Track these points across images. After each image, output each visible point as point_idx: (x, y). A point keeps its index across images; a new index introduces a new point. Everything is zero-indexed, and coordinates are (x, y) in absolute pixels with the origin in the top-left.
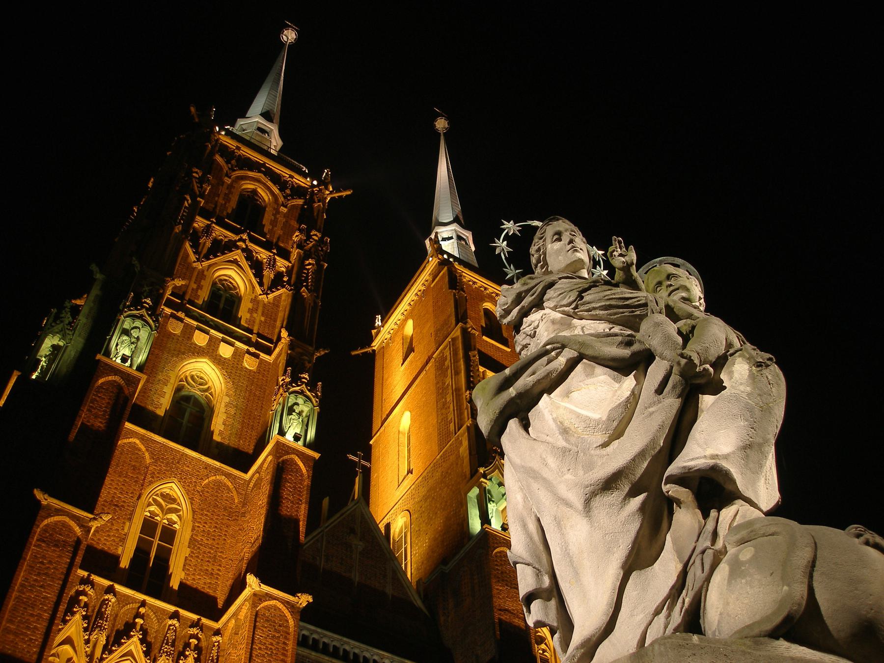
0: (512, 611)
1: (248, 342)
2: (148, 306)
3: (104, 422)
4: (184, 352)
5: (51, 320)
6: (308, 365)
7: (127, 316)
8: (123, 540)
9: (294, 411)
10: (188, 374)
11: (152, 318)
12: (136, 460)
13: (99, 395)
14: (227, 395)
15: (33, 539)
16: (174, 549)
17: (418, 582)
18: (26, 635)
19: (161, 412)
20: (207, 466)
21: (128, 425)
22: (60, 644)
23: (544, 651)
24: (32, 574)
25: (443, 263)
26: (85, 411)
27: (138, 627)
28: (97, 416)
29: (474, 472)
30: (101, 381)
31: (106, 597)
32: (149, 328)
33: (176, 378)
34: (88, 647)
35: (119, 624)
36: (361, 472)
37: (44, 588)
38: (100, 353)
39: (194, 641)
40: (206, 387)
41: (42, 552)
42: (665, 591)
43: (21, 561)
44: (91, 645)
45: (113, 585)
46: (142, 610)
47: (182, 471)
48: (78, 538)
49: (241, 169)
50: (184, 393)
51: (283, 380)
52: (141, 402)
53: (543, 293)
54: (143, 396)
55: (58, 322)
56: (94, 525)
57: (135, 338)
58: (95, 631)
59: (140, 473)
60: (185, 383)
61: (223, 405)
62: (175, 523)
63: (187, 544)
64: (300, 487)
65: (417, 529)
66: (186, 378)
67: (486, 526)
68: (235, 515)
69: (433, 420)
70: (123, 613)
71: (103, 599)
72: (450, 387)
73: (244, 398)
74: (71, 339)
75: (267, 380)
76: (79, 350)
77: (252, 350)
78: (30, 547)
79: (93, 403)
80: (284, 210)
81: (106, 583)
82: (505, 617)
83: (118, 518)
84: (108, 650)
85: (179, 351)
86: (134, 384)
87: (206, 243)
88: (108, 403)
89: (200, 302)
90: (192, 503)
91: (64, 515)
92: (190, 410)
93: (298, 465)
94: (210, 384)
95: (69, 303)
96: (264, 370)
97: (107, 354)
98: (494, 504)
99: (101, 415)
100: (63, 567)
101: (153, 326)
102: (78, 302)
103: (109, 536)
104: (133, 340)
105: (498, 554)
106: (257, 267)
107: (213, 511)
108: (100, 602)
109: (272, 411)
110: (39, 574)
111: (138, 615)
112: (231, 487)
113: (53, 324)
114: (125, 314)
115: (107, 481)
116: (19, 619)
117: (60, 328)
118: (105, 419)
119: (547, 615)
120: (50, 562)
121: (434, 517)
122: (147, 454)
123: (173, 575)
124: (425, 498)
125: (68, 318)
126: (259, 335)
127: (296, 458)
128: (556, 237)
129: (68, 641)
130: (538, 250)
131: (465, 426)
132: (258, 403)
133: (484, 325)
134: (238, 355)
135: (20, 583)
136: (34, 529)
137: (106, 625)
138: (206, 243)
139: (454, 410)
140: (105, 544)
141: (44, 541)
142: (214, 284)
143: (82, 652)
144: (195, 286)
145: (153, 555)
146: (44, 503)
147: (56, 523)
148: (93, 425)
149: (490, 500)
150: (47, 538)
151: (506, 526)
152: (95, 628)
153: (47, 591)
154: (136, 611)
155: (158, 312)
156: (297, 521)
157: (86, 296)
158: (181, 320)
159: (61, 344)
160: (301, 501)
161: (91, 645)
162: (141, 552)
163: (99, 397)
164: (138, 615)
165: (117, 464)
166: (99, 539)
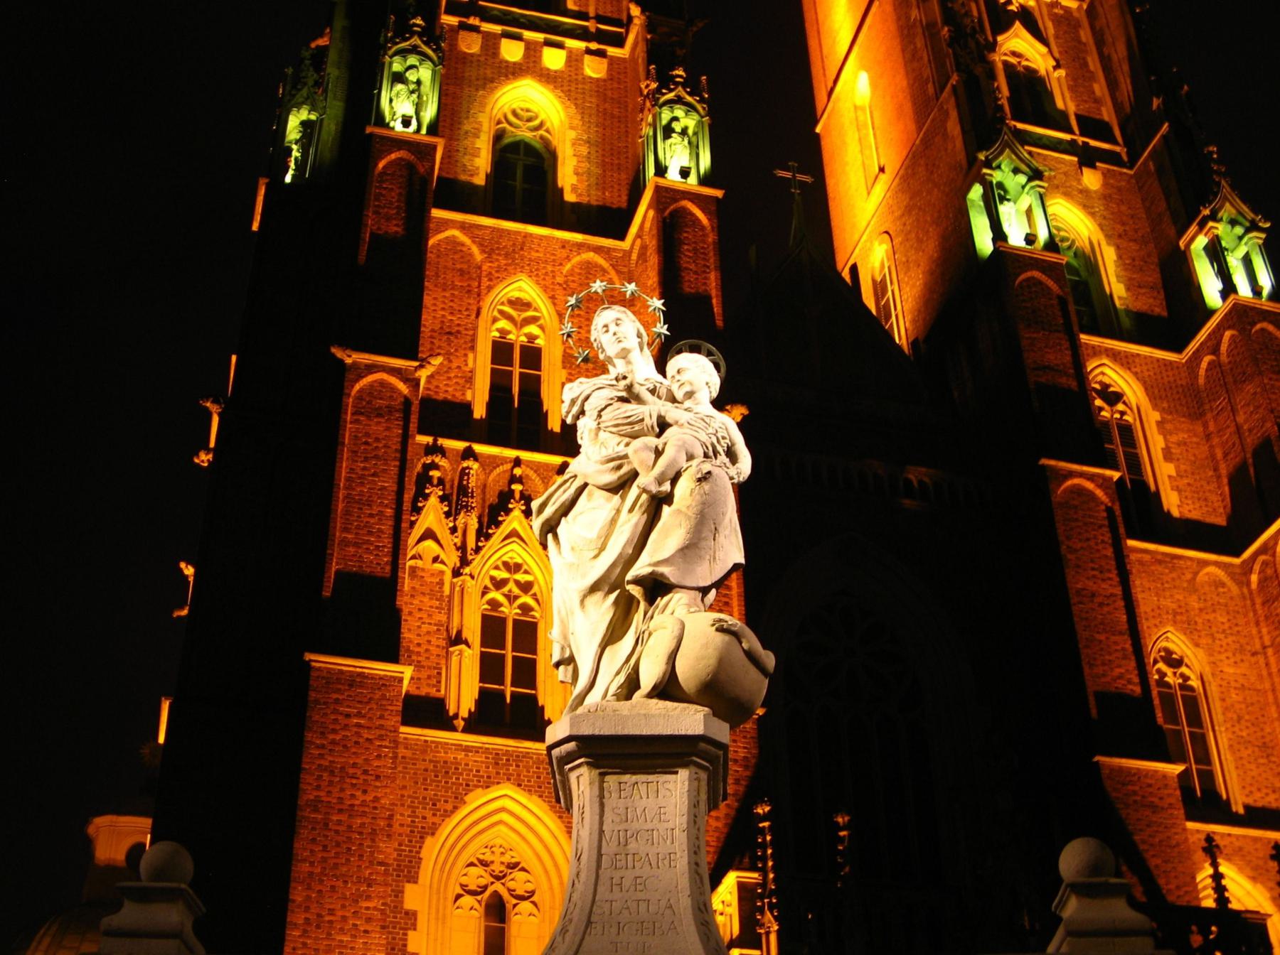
0: (1056, 368)
2: (419, 29)
3: (400, 223)
4: (493, 78)
5: (288, 88)
6: (680, 52)
7: (396, 54)
8: (469, 379)
9: (673, 131)
10: (506, 109)
11: (430, 47)
12: (461, 260)
13: (385, 186)
14: (572, 128)
15: (346, 413)
16: (544, 374)
17: (914, 344)
18: (368, 542)
19: (480, 180)
20: (564, 244)
21: (437, 213)
22: (419, 541)
23: (1123, 413)
24: (357, 461)
26: (370, 214)
27: (517, 496)
28: (388, 219)
29: (972, 160)
30: (381, 165)
31: (465, 464)
32: (430, 63)
33: (490, 122)
34: (456, 537)
35: (491, 496)
36: (799, 194)
37: (378, 477)
38: (370, 124)
40: (536, 123)
41: (363, 429)
42: (624, 659)
43: (340, 447)
44: (460, 533)
45: (470, 447)
46: (518, 471)
47: (530, 260)
48: (406, 398)
50: (507, 140)
51: (647, 86)
52: (448, 173)
53: (583, 405)
54: (449, 162)
55: (299, 87)
56: (423, 374)
57: (414, 83)
58: (460, 513)
59: (471, 279)
60: (505, 125)
61: (568, 145)
62: (537, 337)
63: (559, 364)
64: (703, 248)
65: (904, 259)
66: (506, 117)
67: (999, 243)
69: (902, 81)
70: (493, 480)
71: (460, 468)
72: (918, 24)
73: (597, 126)
74: (325, 107)
75: (626, 87)
76: (340, 120)
77: (594, 46)
78: (346, 426)
79: (378, 200)
81: (460, 445)
83: (456, 350)
84: (483, 534)
85: (485, 79)
86: (430, 155)
88: (400, 194)
90: (554, 304)
91: (379, 371)
93: (692, 214)
94: (542, 116)
95: (307, 51)
96: (619, 73)
97: (381, 121)
98: (1011, 204)
99: (394, 214)
100: (395, 444)
101: (435, 58)
102: (322, 42)
103: (449, 378)
104: (412, 87)
105: (1024, 284)
107: (588, 308)
108: (458, 474)
109: (641, 137)
110: (366, 459)
111: (514, 479)
113: (293, 92)
114: (390, 52)
115: (427, 300)
116: (356, 524)
117: (305, 95)
118: (401, 219)
119: (566, 676)
120: (377, 440)
121: (925, 239)
122: (475, 250)
123: (549, 412)
124: (909, 210)
125: (312, 76)
126: (600, 19)
128: (605, 329)
129: (429, 535)
130: (595, 340)
131: (949, 86)
132: (619, 127)
134: (574, 60)
135: (345, 476)
136: (344, 400)
137: (474, 502)
139: (929, 60)
140: (448, 391)
141: (362, 414)
143: (449, 545)
145: (516, 390)
146: (349, 361)
147: (371, 385)
148: (386, 232)
149: (1003, 199)
150: (364, 407)
151: (1032, 238)
152: (460, 510)
153: (381, 479)
154: (510, 474)
155: (438, 33)
157: (328, 30)
158: (475, 29)
159: (313, 117)
160: (708, 267)
161: (460, 533)
163: (385, 189)
164: (514, 479)
165: (437, 273)
166: (437, 387)
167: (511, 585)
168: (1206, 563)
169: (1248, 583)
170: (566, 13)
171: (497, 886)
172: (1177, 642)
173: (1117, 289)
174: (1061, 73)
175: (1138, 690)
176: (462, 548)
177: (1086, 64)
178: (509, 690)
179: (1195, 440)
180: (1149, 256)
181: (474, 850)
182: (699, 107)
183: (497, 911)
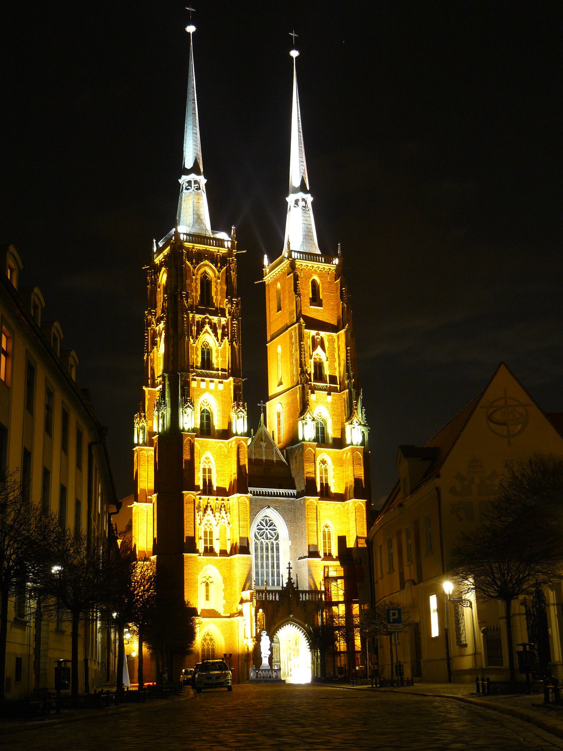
1: (217, 377)
18: (190, 530)
25: (293, 265)
27: (209, 506)
39: (223, 505)
60: (202, 405)
68: (226, 457)
77: (220, 380)
80: (219, 281)
82: (308, 475)
84: (204, 516)
87: (194, 328)
89: (199, 365)
92: (205, 414)
106: (214, 328)
112: (224, 446)
127: (242, 441)
133: (311, 297)
138: (194, 328)
142: (202, 346)
144: (195, 357)
149: (306, 423)
156: (245, 465)
162: (204, 480)
167: (208, 525)
168: (337, 504)
169: (345, 508)
170: (213, 369)
171: (208, 581)
174: (328, 362)
175: (316, 543)
176: (200, 519)
177: (334, 356)
178: (209, 545)
179: (340, 472)
180: (339, 420)
182: (245, 412)
183: (207, 585)
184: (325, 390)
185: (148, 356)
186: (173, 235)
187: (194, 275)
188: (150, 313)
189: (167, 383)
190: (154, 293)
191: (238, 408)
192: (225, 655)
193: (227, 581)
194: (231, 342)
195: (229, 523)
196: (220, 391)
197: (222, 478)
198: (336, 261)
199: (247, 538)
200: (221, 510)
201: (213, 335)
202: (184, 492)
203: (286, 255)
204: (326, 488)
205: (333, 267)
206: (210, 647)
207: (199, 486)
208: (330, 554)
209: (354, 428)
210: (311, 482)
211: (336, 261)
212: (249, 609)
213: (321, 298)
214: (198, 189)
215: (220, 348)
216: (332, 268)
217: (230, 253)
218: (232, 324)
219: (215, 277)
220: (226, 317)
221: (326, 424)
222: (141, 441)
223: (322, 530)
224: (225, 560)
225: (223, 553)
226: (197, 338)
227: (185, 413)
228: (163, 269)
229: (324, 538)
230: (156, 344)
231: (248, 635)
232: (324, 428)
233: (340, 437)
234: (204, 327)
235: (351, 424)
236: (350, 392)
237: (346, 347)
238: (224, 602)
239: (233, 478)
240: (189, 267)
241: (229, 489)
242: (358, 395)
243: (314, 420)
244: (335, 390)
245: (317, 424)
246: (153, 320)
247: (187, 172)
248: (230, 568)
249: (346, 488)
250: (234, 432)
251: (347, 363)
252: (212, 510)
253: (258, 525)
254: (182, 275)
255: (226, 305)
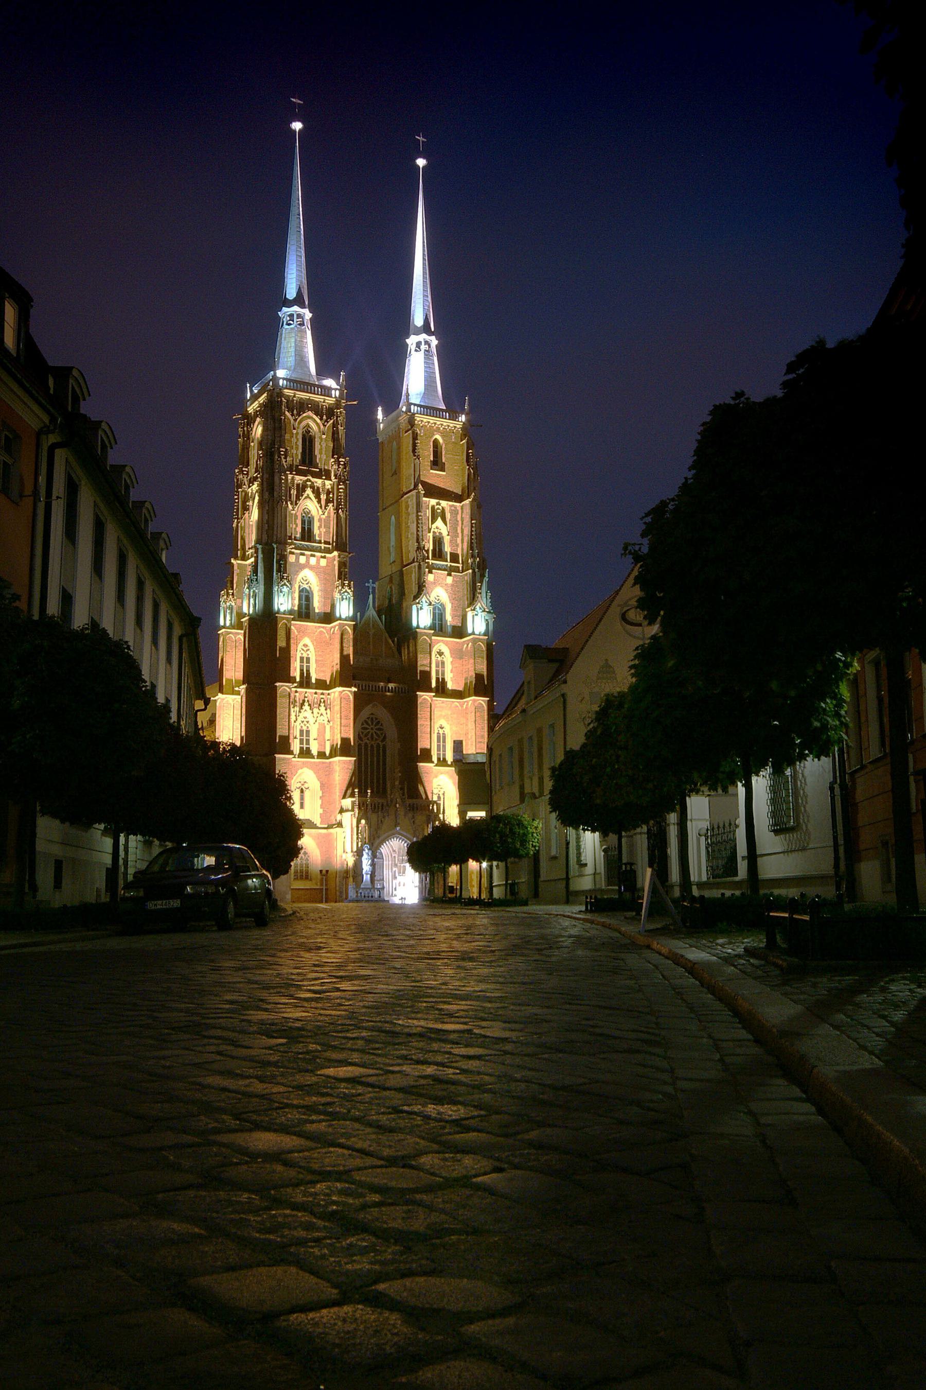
1: (320, 551)
16: (311, 665)
20: (316, 627)
49: (300, 415)
77: (323, 555)
80: (324, 437)
82: (422, 668)
84: (300, 712)
87: (294, 492)
89: (298, 536)
92: (304, 594)
126: (326, 543)
133: (432, 459)
134: (318, 561)
138: (294, 492)
144: (294, 526)
149: (421, 608)
158: (293, 553)
162: (302, 670)
164: (305, 697)
167: (305, 722)
170: (315, 542)
172: (443, 722)
173: (449, 618)
174: (449, 537)
178: (305, 746)
181: (299, 780)
183: (302, 791)
184: (445, 570)
185: (238, 523)
186: (271, 380)
187: (294, 429)
188: (241, 472)
189: (260, 556)
190: (246, 448)
191: (343, 587)
192: (321, 871)
193: (325, 787)
194: (337, 509)
195: (328, 721)
196: (323, 567)
197: (322, 669)
198: (463, 418)
199: (349, 739)
200: (319, 705)
201: (315, 500)
202: (277, 684)
203: (404, 409)
204: (442, 684)
205: (459, 425)
206: (304, 862)
207: (295, 678)
208: (444, 759)
209: (476, 615)
210: (427, 675)
211: (463, 418)
212: (349, 820)
213: (443, 461)
214: (302, 324)
215: (324, 517)
216: (458, 426)
217: (338, 405)
218: (338, 489)
219: (320, 432)
220: (331, 480)
221: (444, 609)
222: (228, 624)
223: (436, 731)
224: (323, 763)
225: (321, 755)
226: (296, 504)
227: (281, 592)
228: (258, 419)
229: (439, 741)
230: (248, 509)
231: (348, 849)
232: (442, 614)
233: (460, 625)
234: (305, 491)
235: (474, 610)
236: (474, 572)
237: (472, 520)
238: (321, 811)
239: (335, 669)
240: (289, 419)
241: (330, 682)
242: (483, 576)
243: (430, 604)
244: (456, 570)
245: (434, 609)
246: (245, 480)
247: (289, 303)
248: (329, 771)
249: (466, 684)
250: (338, 615)
251: (471, 539)
252: (309, 705)
253: (363, 724)
254: (280, 428)
255: (331, 465)
